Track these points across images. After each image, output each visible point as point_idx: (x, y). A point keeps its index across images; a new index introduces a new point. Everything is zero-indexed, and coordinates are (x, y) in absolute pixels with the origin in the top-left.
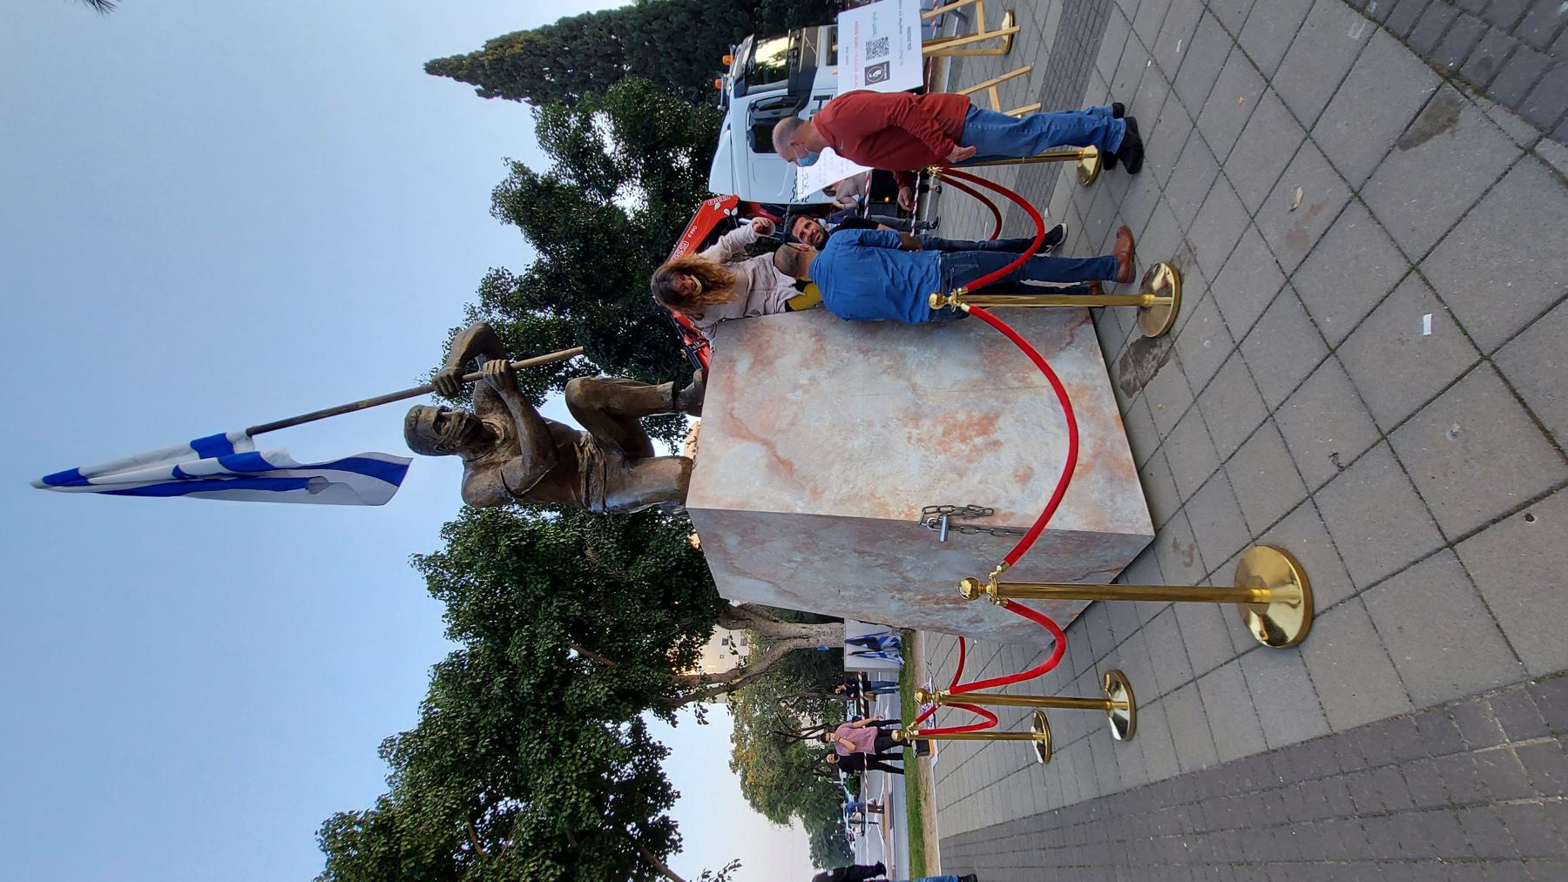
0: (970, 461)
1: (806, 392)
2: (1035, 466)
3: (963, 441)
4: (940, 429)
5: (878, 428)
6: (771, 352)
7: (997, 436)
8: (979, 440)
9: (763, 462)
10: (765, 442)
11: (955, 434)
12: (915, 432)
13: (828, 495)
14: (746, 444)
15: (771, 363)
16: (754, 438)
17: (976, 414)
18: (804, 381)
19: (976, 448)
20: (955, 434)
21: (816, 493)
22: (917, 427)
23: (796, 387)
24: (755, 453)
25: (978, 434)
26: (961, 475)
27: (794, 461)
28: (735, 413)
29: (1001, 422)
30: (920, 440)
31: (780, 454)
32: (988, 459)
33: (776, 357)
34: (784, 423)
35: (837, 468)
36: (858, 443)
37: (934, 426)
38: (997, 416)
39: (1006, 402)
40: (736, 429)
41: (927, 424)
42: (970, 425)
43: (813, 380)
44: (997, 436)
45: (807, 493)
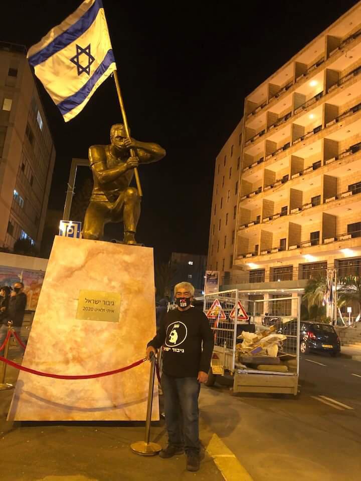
0: (60, 350)
1: (107, 285)
3: (71, 349)
4: (79, 340)
6: (132, 270)
9: (73, 266)
10: (83, 267)
11: (75, 346)
12: (79, 329)
13: (52, 291)
16: (86, 262)
18: (113, 284)
20: (75, 346)
21: (54, 286)
22: (81, 330)
23: (110, 280)
28: (101, 254)
30: (74, 330)
31: (76, 273)
33: (129, 272)
34: (92, 274)
35: (65, 295)
37: (81, 338)
38: (82, 365)
40: (91, 254)
41: (82, 334)
42: (79, 353)
43: (114, 287)
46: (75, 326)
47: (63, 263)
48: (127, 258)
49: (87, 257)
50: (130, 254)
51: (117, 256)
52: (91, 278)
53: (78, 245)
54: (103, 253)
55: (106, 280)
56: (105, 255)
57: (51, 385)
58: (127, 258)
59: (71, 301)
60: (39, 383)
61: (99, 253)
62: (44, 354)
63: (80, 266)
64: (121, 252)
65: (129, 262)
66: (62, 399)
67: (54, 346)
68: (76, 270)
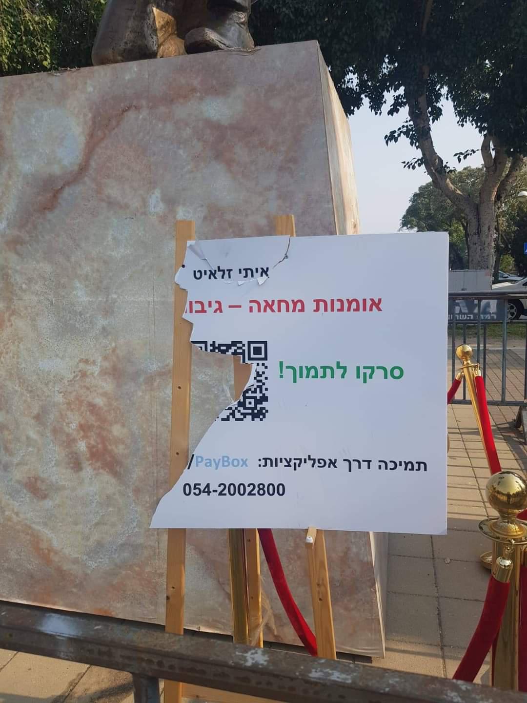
0: (55, 431)
1: (163, 219)
2: (48, 504)
3: (81, 427)
4: (100, 401)
5: (101, 322)
6: (241, 153)
7: (88, 471)
8: (82, 446)
9: (56, 170)
10: (83, 168)
11: (92, 420)
12: (96, 370)
14: (82, 140)
15: (218, 156)
17: (120, 450)
18: (181, 213)
19: (70, 442)
20: (92, 420)
22: (104, 372)
23: (171, 202)
24: (69, 155)
25: (90, 448)
26: (37, 417)
27: (57, 212)
29: (106, 477)
30: (84, 375)
31: (67, 192)
32: (56, 452)
33: (229, 163)
34: (113, 190)
36: (81, 295)
37: (105, 394)
38: (115, 474)
39: (137, 491)
40: (105, 121)
41: (108, 385)
42: (104, 440)
44: (88, 471)
45: (16, 232)
46: (86, 362)
47: (26, 167)
48: (216, 109)
49: (91, 135)
50: (220, 87)
51: (181, 111)
52: (112, 204)
53: (61, 98)
54: (138, 108)
55: (156, 203)
56: (144, 114)
57: (45, 524)
58: (216, 109)
59: (64, 287)
60: (17, 514)
61: (124, 111)
62: (18, 440)
63: (76, 168)
64: (194, 90)
65: (225, 122)
66: (76, 561)
67: (37, 417)
68: (68, 184)
